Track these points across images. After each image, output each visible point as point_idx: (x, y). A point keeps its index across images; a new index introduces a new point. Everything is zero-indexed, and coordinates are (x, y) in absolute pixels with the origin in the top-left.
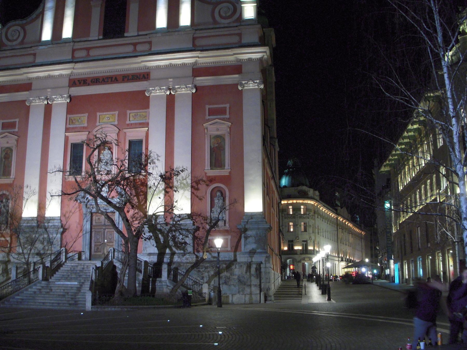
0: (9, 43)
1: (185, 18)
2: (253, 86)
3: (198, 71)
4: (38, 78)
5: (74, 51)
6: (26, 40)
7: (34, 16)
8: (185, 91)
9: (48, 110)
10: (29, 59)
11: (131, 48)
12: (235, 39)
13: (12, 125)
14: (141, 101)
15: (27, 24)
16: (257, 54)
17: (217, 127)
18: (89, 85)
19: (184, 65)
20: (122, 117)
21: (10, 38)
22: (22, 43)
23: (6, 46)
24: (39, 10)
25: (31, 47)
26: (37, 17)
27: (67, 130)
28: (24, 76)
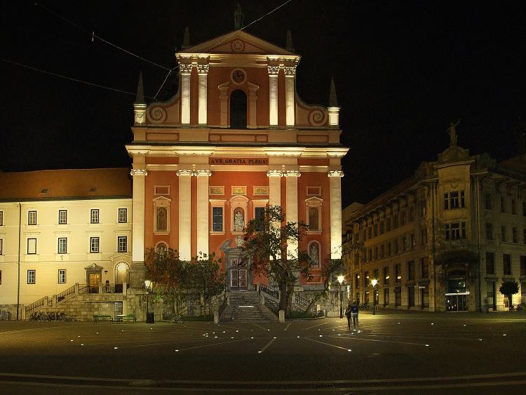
0: (154, 121)
1: (290, 120)
2: (337, 175)
3: (301, 161)
4: (185, 156)
5: (209, 135)
6: (167, 121)
7: (173, 100)
8: (293, 175)
9: (194, 182)
10: (173, 138)
11: (252, 139)
12: (325, 140)
13: (165, 191)
14: (263, 179)
15: (168, 107)
16: (341, 152)
17: (310, 202)
18: (224, 164)
19: (293, 157)
20: (250, 190)
21: (155, 117)
22: (164, 122)
23: (150, 123)
24: (177, 96)
25: (176, 128)
26: (176, 103)
27: (210, 197)
28: (173, 152)
